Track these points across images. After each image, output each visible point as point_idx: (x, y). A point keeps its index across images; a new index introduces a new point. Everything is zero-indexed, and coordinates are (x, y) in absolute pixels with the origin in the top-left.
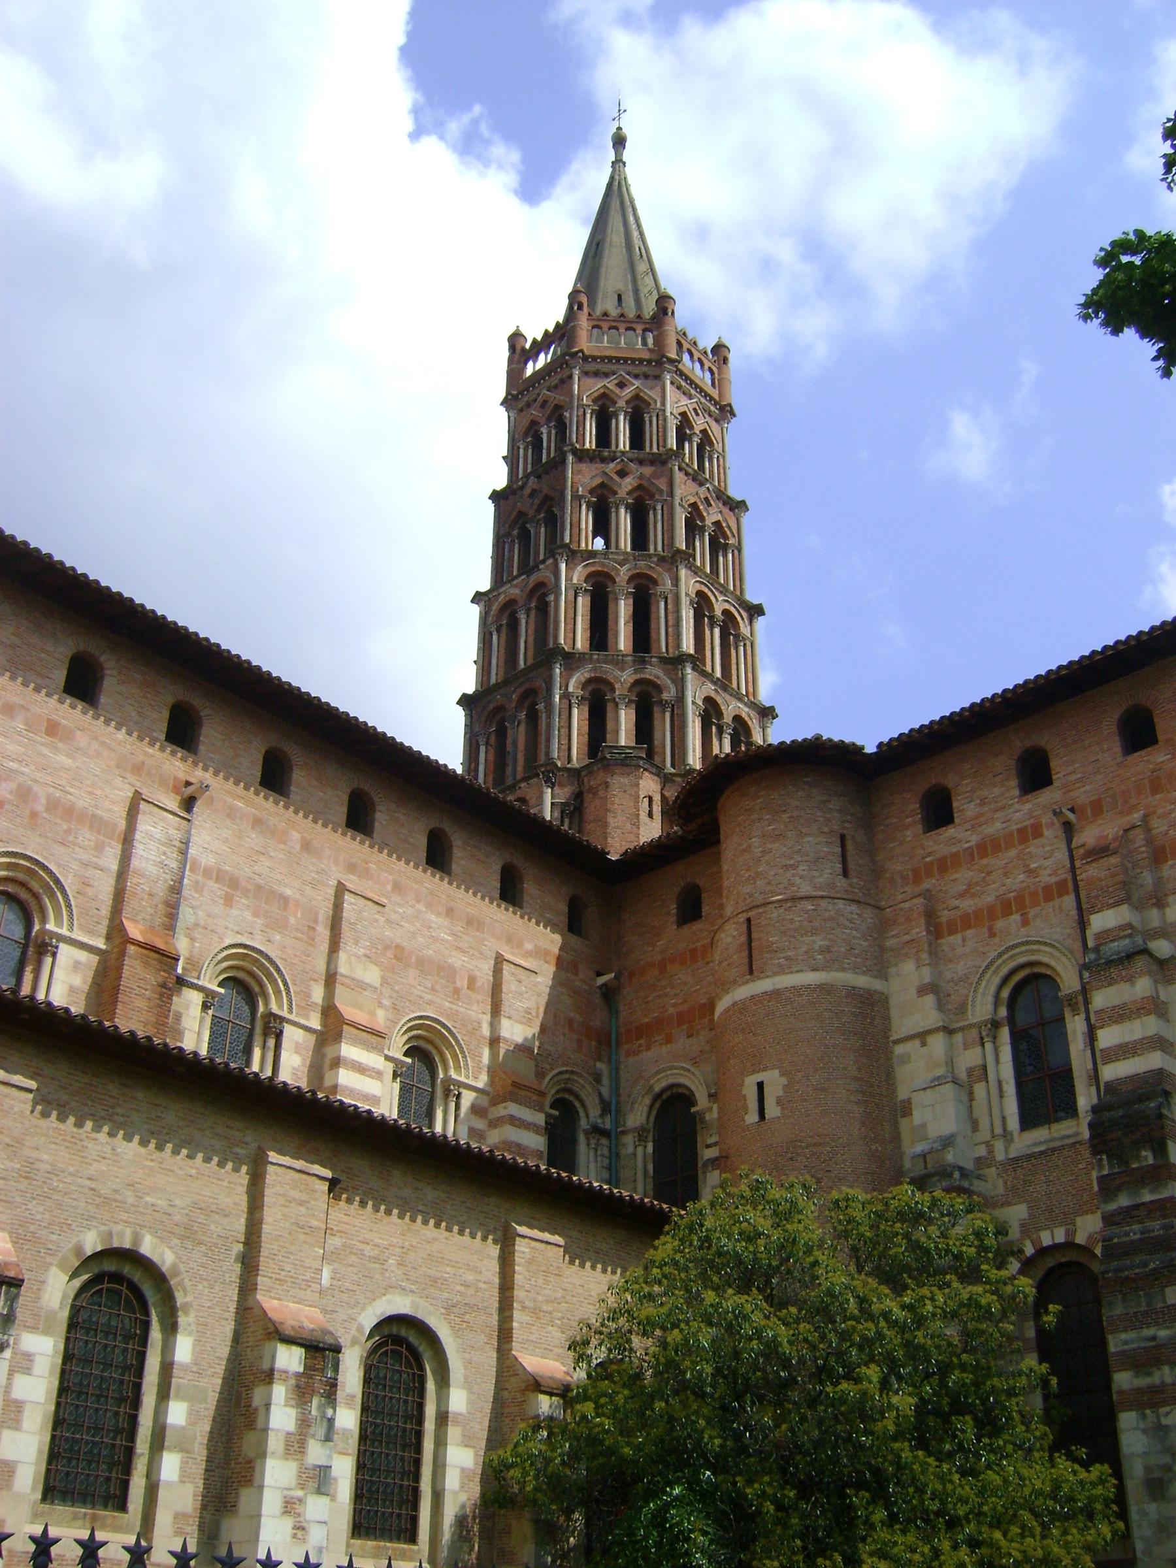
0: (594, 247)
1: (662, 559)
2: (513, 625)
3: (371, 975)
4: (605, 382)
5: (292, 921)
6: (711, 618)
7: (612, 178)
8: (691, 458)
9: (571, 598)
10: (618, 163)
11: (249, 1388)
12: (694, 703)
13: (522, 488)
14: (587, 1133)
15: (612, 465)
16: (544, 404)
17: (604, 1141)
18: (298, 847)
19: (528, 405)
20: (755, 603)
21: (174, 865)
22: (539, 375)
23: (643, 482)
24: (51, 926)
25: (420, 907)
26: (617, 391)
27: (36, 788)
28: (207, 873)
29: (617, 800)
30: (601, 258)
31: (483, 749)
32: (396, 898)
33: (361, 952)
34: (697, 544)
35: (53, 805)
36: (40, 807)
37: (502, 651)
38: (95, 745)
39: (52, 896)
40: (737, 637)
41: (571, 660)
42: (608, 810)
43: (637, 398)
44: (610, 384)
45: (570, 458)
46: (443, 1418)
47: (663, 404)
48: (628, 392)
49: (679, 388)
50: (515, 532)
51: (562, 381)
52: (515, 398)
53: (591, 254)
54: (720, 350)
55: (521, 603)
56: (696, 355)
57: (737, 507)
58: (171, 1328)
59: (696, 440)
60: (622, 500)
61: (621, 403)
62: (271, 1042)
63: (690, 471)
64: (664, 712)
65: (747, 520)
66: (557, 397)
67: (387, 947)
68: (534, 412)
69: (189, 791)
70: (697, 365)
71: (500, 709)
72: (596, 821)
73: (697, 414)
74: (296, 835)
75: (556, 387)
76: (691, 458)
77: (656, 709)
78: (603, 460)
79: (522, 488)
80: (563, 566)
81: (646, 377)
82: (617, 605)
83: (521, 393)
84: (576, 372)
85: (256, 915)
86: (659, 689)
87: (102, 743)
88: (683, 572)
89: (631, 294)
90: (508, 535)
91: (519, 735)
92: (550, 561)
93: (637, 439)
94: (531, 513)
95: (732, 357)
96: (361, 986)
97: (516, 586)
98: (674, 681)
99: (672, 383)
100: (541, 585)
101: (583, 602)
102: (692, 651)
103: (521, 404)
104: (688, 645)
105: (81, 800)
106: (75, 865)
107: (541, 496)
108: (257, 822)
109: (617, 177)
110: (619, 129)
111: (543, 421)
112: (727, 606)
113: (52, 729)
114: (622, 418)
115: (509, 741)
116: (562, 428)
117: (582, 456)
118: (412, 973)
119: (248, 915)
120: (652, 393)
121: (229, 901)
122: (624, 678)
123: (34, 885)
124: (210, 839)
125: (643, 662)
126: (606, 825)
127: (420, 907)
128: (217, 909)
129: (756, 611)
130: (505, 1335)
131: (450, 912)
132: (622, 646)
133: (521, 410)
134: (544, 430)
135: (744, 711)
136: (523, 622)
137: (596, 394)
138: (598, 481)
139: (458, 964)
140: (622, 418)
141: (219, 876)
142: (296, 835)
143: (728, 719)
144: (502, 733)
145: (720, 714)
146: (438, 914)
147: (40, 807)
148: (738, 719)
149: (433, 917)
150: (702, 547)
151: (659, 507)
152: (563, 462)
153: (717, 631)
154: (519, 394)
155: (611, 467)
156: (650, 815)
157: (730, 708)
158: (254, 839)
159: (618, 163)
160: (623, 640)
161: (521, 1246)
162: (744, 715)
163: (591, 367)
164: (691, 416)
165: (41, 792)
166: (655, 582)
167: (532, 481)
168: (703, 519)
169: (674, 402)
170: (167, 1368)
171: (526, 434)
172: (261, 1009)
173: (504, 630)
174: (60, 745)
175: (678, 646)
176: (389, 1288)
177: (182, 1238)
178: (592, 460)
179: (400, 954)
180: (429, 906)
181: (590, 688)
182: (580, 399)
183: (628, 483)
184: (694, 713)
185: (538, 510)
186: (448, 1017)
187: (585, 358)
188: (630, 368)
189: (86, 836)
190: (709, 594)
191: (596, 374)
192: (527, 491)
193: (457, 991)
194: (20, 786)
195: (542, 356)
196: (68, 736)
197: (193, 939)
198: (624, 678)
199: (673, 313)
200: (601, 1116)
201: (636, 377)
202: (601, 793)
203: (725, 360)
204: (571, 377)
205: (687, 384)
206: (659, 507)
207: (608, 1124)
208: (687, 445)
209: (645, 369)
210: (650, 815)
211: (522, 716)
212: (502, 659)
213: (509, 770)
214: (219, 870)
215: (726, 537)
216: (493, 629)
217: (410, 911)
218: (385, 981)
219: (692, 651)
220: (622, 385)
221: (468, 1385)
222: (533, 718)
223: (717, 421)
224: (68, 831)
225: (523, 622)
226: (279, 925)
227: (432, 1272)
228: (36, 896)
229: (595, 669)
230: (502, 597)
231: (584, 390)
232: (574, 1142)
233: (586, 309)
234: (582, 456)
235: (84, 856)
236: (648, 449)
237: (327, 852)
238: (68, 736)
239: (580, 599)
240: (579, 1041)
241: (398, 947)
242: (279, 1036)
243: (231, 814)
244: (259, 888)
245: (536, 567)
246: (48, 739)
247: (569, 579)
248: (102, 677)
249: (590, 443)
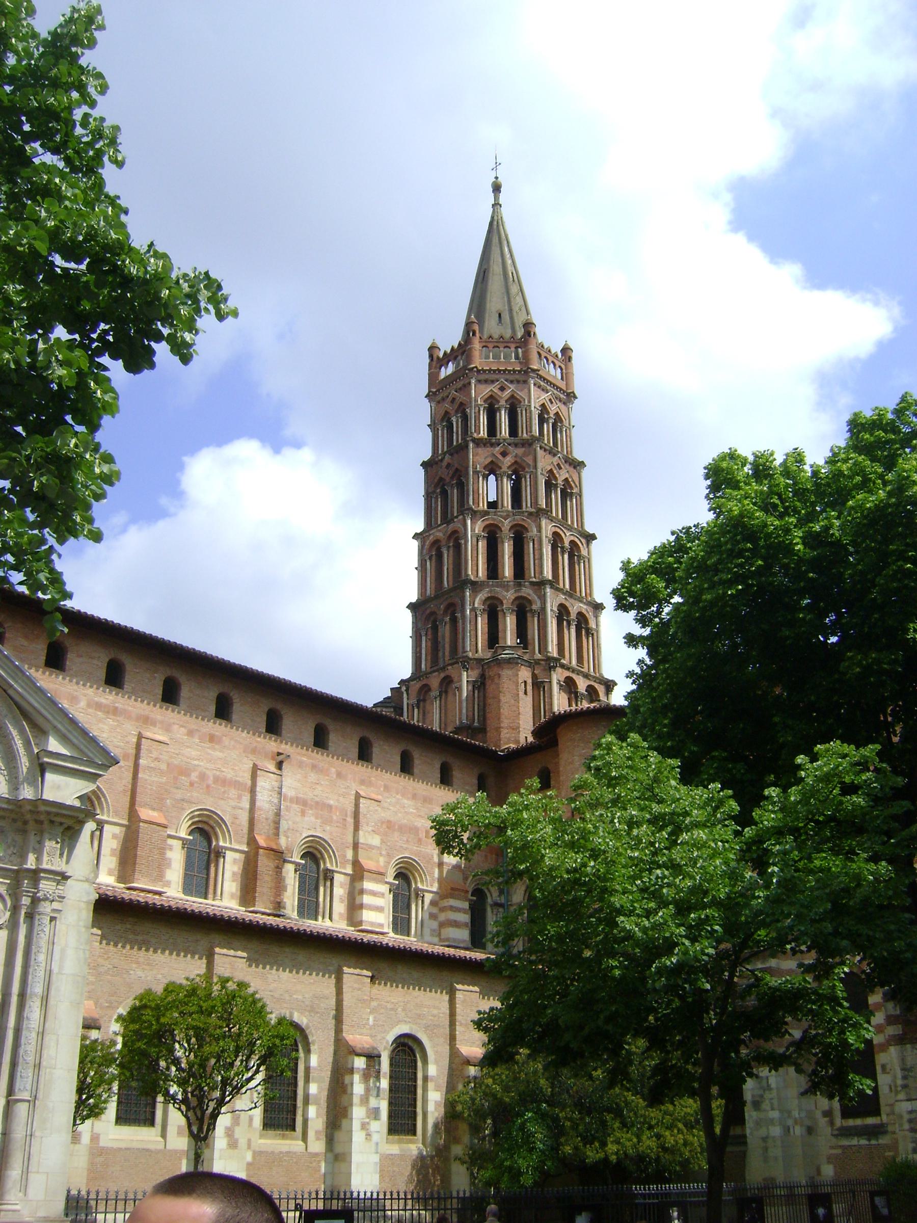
0: (482, 273)
1: (531, 514)
2: (440, 556)
3: (376, 841)
4: (491, 387)
5: (335, 818)
6: (562, 548)
7: (492, 217)
8: (549, 440)
10: (496, 205)
11: (342, 1076)
12: (552, 610)
13: (442, 460)
14: (491, 906)
15: (497, 449)
16: (454, 399)
17: (501, 910)
18: (335, 776)
19: (443, 399)
20: (591, 532)
21: (276, 801)
22: (450, 379)
23: (518, 460)
24: (221, 843)
25: (399, 797)
26: (499, 393)
27: (208, 772)
28: (292, 800)
30: (487, 282)
31: (424, 638)
32: (386, 794)
33: (370, 829)
34: (553, 496)
35: (217, 779)
36: (210, 782)
37: (433, 573)
38: (232, 743)
39: (220, 827)
40: (579, 556)
41: (476, 586)
43: (512, 397)
44: (494, 388)
45: (471, 445)
46: (426, 1079)
47: (529, 402)
48: (507, 394)
49: (539, 387)
50: (438, 490)
51: (464, 386)
52: (435, 393)
53: (480, 279)
54: (566, 350)
55: (443, 543)
56: (550, 359)
57: (578, 465)
58: (308, 1051)
59: (551, 421)
60: (505, 472)
61: (503, 402)
62: (328, 883)
63: (547, 448)
64: (533, 617)
65: (585, 473)
66: (461, 397)
67: (383, 823)
68: (447, 405)
69: (280, 758)
70: (552, 365)
71: (433, 613)
72: (494, 698)
73: (552, 403)
74: (333, 770)
75: (460, 389)
76: (549, 440)
77: (529, 615)
78: (492, 445)
79: (442, 460)
80: (469, 522)
81: (518, 382)
82: (503, 545)
83: (438, 390)
84: (473, 381)
85: (317, 818)
86: (530, 602)
87: (236, 741)
88: (544, 522)
89: (507, 313)
90: (434, 492)
91: (445, 631)
92: (461, 517)
93: (513, 431)
94: (448, 480)
95: (574, 355)
96: (371, 847)
97: (440, 531)
98: (539, 598)
99: (535, 385)
100: (455, 532)
101: (482, 545)
102: (550, 578)
103: (439, 398)
104: (548, 573)
105: (229, 774)
106: (229, 809)
107: (454, 469)
108: (314, 767)
109: (496, 218)
110: (497, 178)
111: (452, 412)
112: (572, 538)
113: (212, 739)
114: (503, 412)
115: (439, 634)
116: (465, 419)
117: (478, 442)
118: (396, 834)
119: (313, 819)
120: (522, 394)
121: (303, 813)
122: (508, 596)
123: (211, 822)
124: (292, 781)
125: (520, 585)
126: (499, 701)
127: (399, 797)
128: (298, 819)
129: (590, 538)
130: (452, 1038)
131: (414, 797)
132: (507, 574)
133: (439, 402)
134: (454, 419)
135: (584, 608)
136: (446, 556)
137: (486, 397)
138: (489, 460)
139: (419, 825)
140: (503, 412)
141: (297, 800)
142: (333, 770)
143: (573, 616)
144: (435, 628)
145: (568, 613)
146: (408, 799)
147: (210, 782)
148: (580, 614)
149: (406, 801)
150: (557, 497)
151: (528, 476)
152: (467, 446)
153: (566, 556)
154: (437, 391)
156: (526, 693)
157: (575, 608)
158: (313, 777)
159: (496, 205)
160: (507, 570)
161: (459, 995)
162: (584, 611)
163: (483, 377)
164: (548, 404)
165: (210, 774)
166: (526, 529)
167: (447, 457)
168: (556, 479)
169: (536, 398)
170: (307, 1069)
171: (442, 420)
172: (322, 866)
173: (434, 558)
174: (217, 747)
175: (541, 572)
176: (399, 1022)
177: (309, 1011)
178: (485, 445)
179: (390, 825)
180: (403, 795)
181: (488, 603)
182: (476, 401)
183: (508, 461)
184: (552, 617)
185: (452, 478)
186: (416, 855)
187: (478, 371)
188: (507, 377)
189: (233, 793)
190: (561, 533)
191: (486, 381)
192: (445, 464)
193: (420, 840)
194: (200, 773)
196: (219, 741)
197: (288, 837)
198: (508, 596)
199: (534, 334)
200: (499, 896)
201: (512, 382)
202: (496, 681)
203: (570, 359)
204: (470, 383)
205: (545, 383)
206: (528, 476)
207: (502, 900)
208: (545, 426)
209: (517, 377)
210: (526, 693)
211: (447, 619)
212: (433, 578)
213: (440, 654)
214: (297, 798)
215: (571, 488)
216: (427, 558)
217: (393, 800)
218: (382, 841)
219: (550, 578)
220: (502, 389)
221: (436, 1062)
222: (454, 620)
223: (564, 403)
224: (224, 792)
225: (446, 556)
226: (327, 821)
227: (418, 1012)
228: (213, 828)
229: (490, 591)
230: (432, 537)
231: (478, 393)
232: (485, 911)
233: (478, 335)
234: (478, 442)
235: (233, 803)
236: (520, 434)
237: (350, 776)
238: (219, 741)
239: (480, 543)
240: (486, 856)
241: (389, 822)
242: (332, 880)
243: (301, 765)
244: (317, 803)
245: (452, 521)
246: (210, 745)
247: (473, 530)
248: (232, 704)
249: (483, 433)
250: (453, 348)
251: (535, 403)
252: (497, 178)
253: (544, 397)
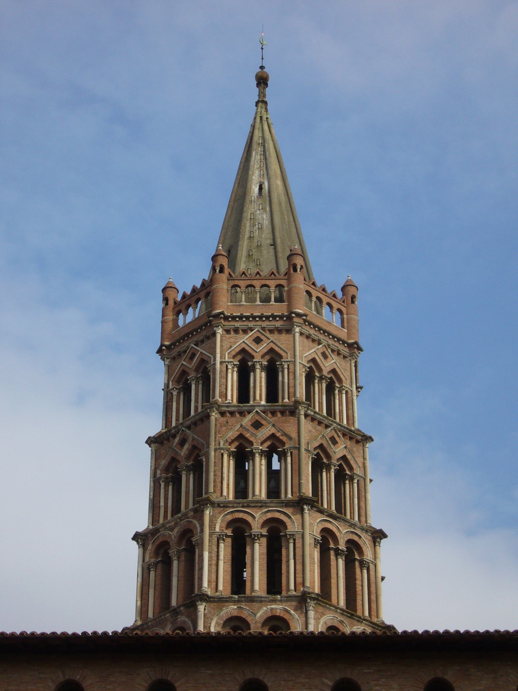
26: (254, 346)
48: (262, 348)
49: (308, 337)
84: (220, 331)
99: (301, 334)
110: (262, 67)
154: (172, 349)
164: (320, 359)
169: (300, 352)
195: (191, 310)
204: (214, 334)
205: (318, 333)
250: (194, 290)
251: (301, 358)
252: (262, 67)
253: (313, 351)
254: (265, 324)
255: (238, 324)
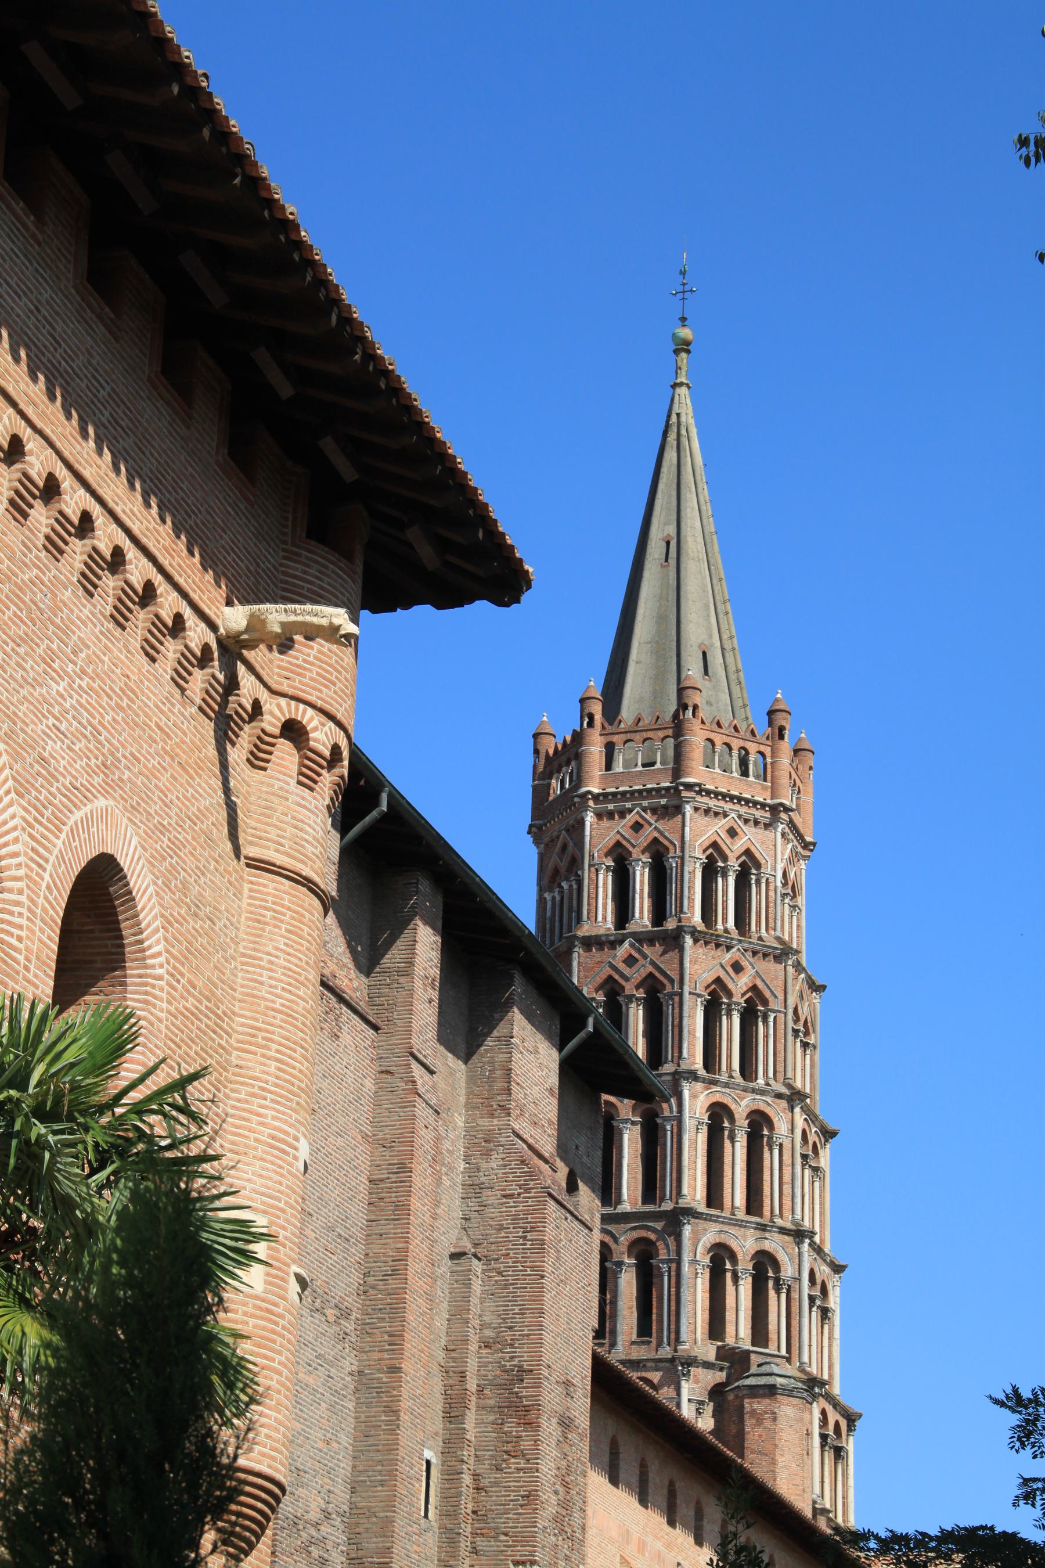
9: (693, 1134)
26: (728, 840)
29: (784, 1435)
42: (776, 1446)
43: (748, 852)
44: (720, 826)
45: (688, 940)
81: (756, 823)
86: (776, 1265)
122: (745, 1244)
155: (728, 957)
160: (736, 1193)
166: (771, 1127)
191: (707, 811)
198: (745, 1244)
202: (768, 1423)
206: (771, 1019)
254: (743, 810)
255: (712, 803)
